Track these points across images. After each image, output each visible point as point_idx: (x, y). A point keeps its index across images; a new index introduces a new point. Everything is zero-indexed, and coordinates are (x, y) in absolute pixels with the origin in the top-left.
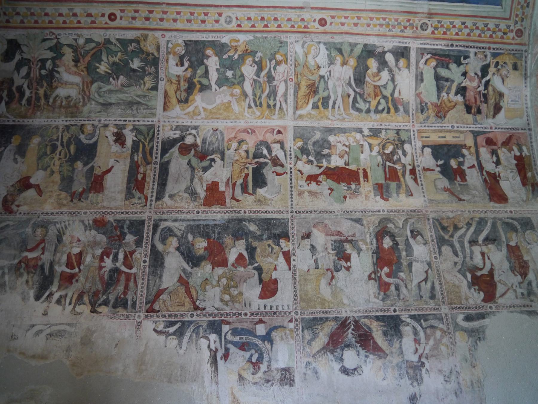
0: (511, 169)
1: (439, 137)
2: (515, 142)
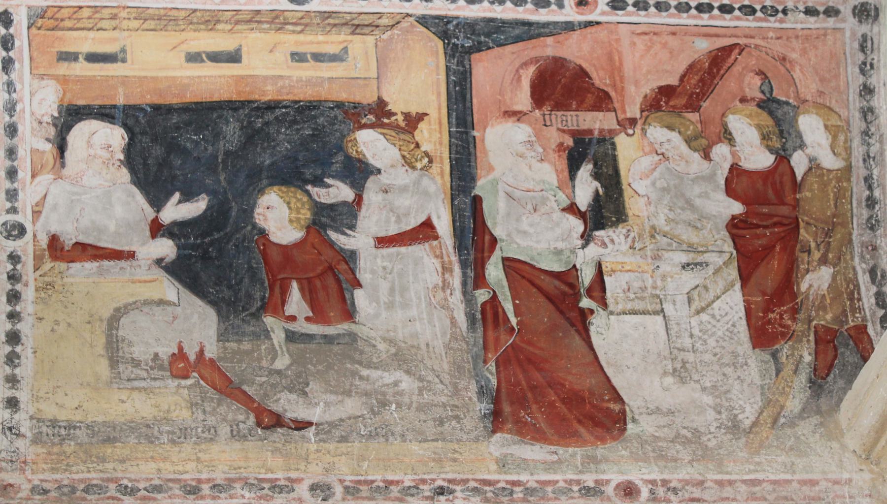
0: (691, 248)
1: (194, 58)
2: (753, 86)
